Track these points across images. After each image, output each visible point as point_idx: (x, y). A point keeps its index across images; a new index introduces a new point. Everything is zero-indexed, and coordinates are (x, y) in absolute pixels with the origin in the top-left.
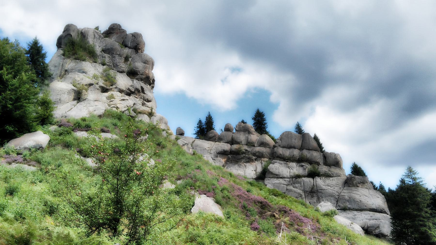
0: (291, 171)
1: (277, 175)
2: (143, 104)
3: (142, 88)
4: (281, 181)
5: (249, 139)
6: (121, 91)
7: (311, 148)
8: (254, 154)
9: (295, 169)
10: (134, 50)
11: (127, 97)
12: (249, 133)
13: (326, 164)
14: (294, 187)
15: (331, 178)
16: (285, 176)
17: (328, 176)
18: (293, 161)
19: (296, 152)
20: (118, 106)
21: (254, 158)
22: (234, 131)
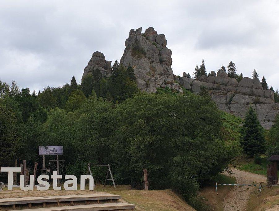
0: (245, 100)
1: (237, 102)
2: (168, 77)
3: (167, 69)
4: (239, 106)
5: (224, 82)
6: (159, 75)
7: (257, 88)
8: (226, 90)
9: (248, 99)
10: (161, 46)
11: (161, 77)
12: (225, 77)
13: (265, 96)
14: (245, 109)
15: (266, 105)
16: (241, 103)
17: (264, 103)
18: (246, 95)
19: (248, 90)
20: (159, 83)
21: (226, 92)
22: (216, 76)
